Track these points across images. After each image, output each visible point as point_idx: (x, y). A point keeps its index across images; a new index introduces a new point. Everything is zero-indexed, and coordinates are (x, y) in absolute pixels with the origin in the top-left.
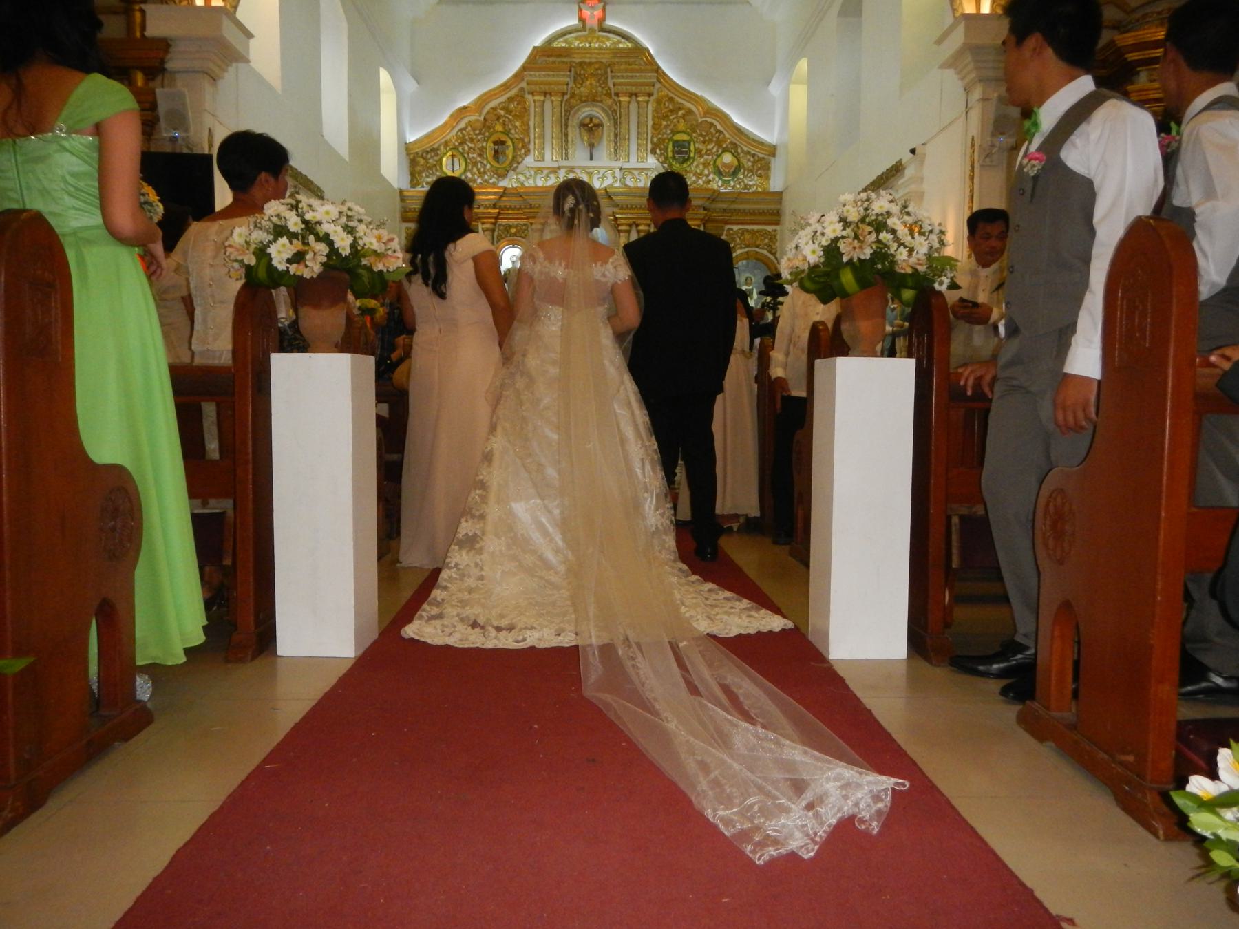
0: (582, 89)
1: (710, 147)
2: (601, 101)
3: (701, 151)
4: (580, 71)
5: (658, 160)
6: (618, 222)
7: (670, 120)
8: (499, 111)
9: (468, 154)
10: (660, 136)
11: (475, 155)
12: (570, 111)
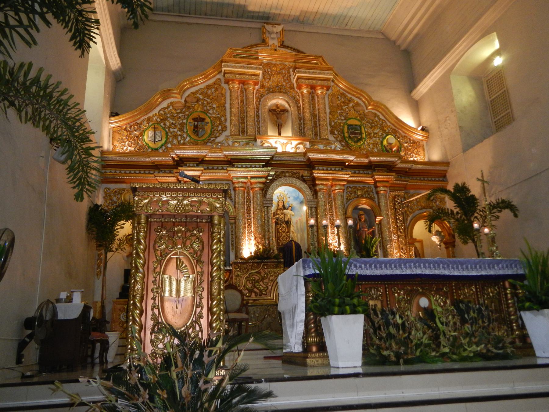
0: (270, 83)
1: (375, 131)
2: (285, 93)
3: (369, 134)
4: (268, 70)
5: (336, 138)
6: (317, 182)
7: (342, 109)
8: (198, 95)
9: (169, 130)
10: (336, 121)
11: (176, 130)
12: (260, 99)
